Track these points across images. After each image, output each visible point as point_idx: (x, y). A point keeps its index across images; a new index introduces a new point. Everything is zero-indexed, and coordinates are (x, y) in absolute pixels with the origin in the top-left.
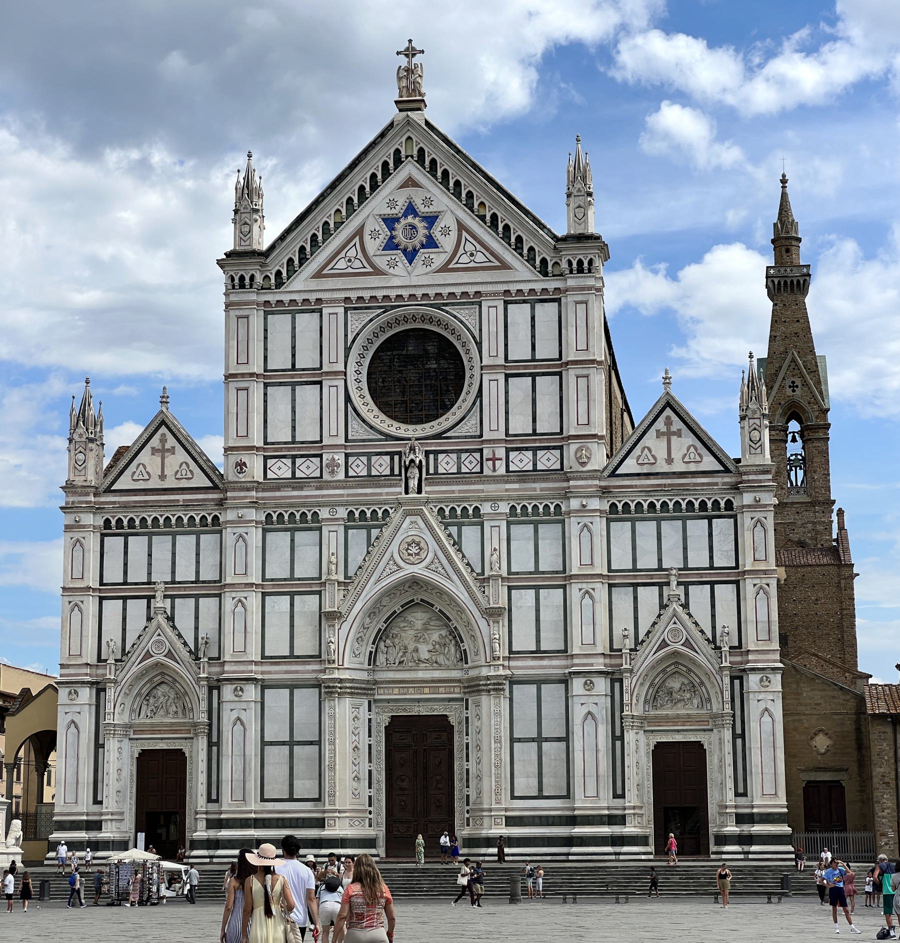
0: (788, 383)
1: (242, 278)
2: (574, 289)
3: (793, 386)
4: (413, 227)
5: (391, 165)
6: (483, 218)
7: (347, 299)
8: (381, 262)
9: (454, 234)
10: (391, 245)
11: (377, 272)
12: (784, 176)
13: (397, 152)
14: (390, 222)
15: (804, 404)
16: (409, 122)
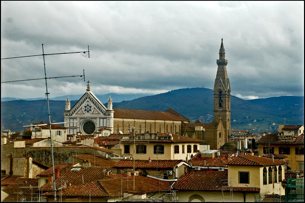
0: (219, 85)
1: (66, 114)
2: (108, 117)
3: (220, 86)
4: (88, 108)
5: (85, 99)
6: (97, 107)
7: (80, 117)
8: (84, 113)
9: (93, 109)
10: (85, 110)
11: (84, 114)
12: (222, 39)
13: (86, 97)
14: (85, 107)
15: (222, 89)
16: (87, 93)
